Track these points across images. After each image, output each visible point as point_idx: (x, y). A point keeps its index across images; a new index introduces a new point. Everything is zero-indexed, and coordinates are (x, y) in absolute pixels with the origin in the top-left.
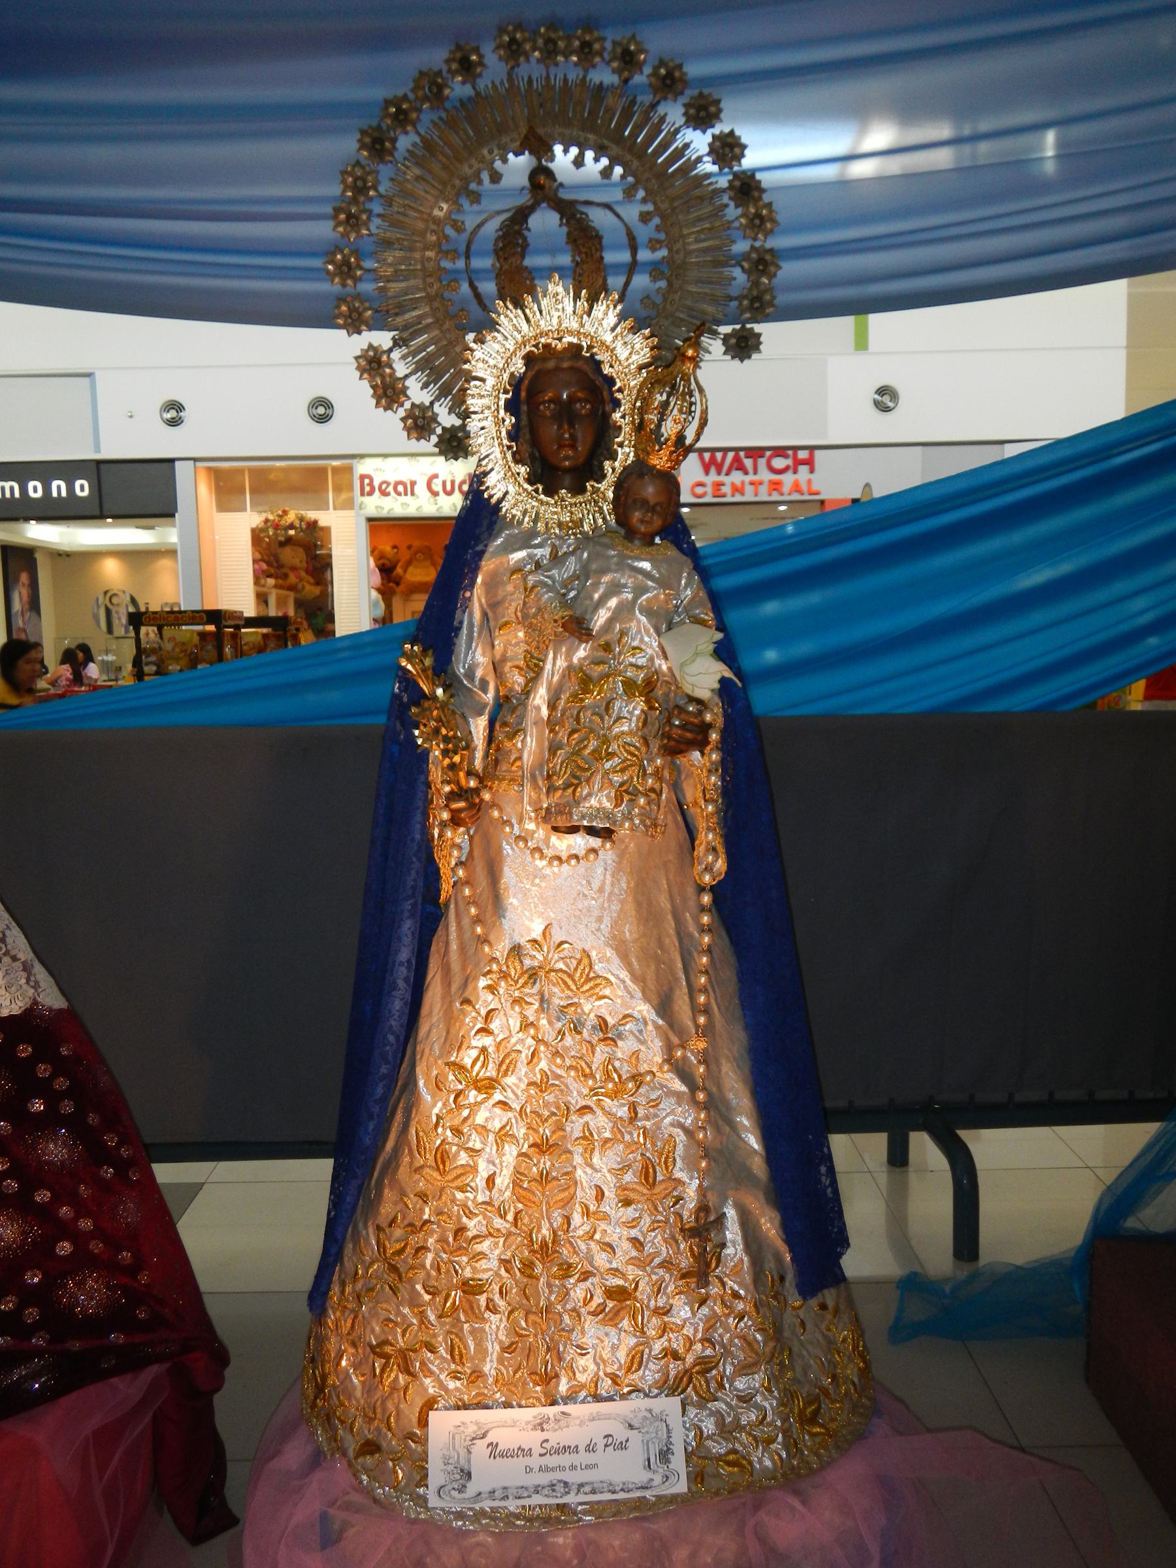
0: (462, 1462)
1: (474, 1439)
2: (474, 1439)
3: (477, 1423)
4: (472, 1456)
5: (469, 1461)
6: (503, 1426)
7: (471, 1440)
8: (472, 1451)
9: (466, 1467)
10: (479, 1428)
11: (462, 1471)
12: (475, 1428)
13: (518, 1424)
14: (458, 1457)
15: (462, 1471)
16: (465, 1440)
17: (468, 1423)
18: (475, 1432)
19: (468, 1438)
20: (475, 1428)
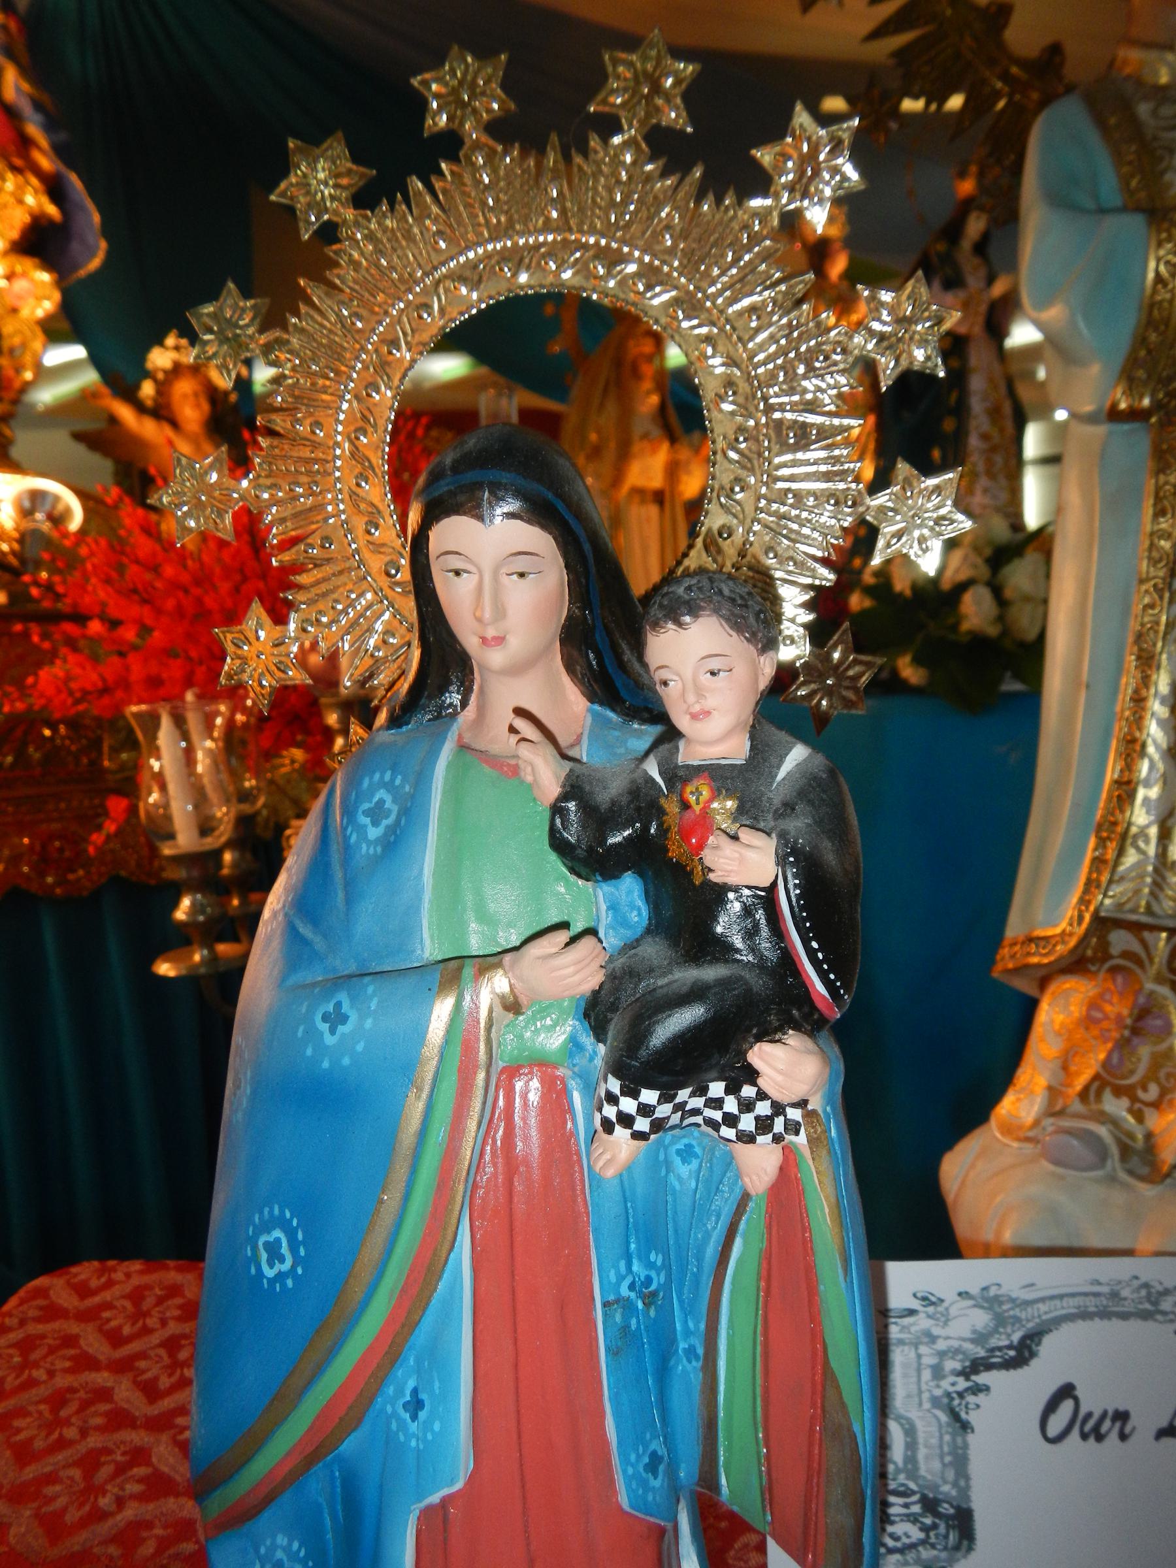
0: (930, 1467)
1: (976, 1366)
2: (976, 1366)
3: (989, 1300)
4: (970, 1438)
5: (960, 1462)
6: (1105, 1314)
7: (965, 1374)
8: (972, 1417)
9: (946, 1488)
10: (1001, 1321)
11: (930, 1505)
12: (981, 1319)
13: (1166, 1305)
14: (911, 1445)
15: (930, 1505)
16: (938, 1373)
17: (949, 1296)
18: (979, 1338)
19: (951, 1365)
20: (981, 1319)
